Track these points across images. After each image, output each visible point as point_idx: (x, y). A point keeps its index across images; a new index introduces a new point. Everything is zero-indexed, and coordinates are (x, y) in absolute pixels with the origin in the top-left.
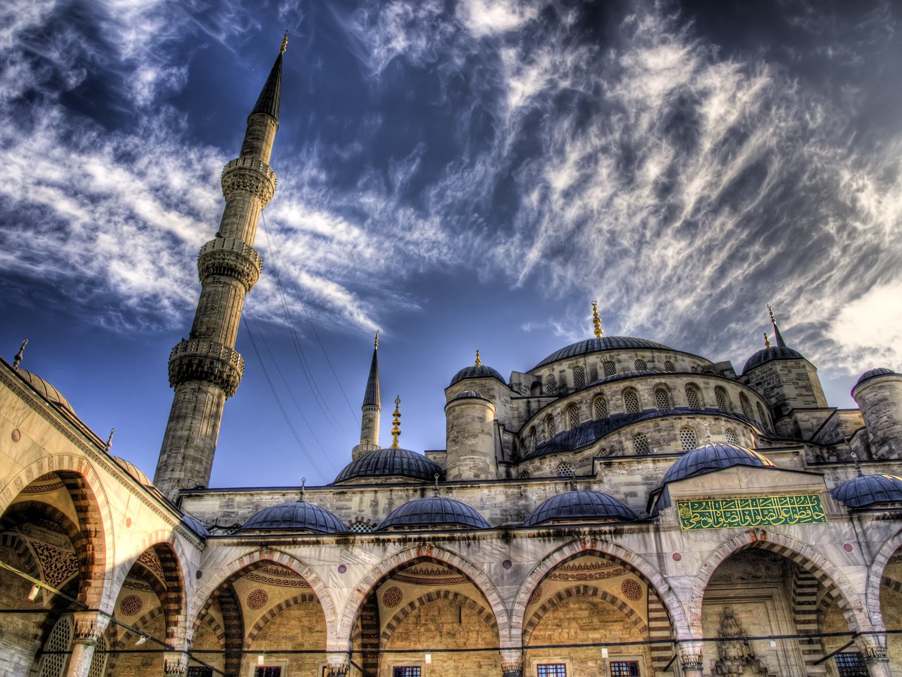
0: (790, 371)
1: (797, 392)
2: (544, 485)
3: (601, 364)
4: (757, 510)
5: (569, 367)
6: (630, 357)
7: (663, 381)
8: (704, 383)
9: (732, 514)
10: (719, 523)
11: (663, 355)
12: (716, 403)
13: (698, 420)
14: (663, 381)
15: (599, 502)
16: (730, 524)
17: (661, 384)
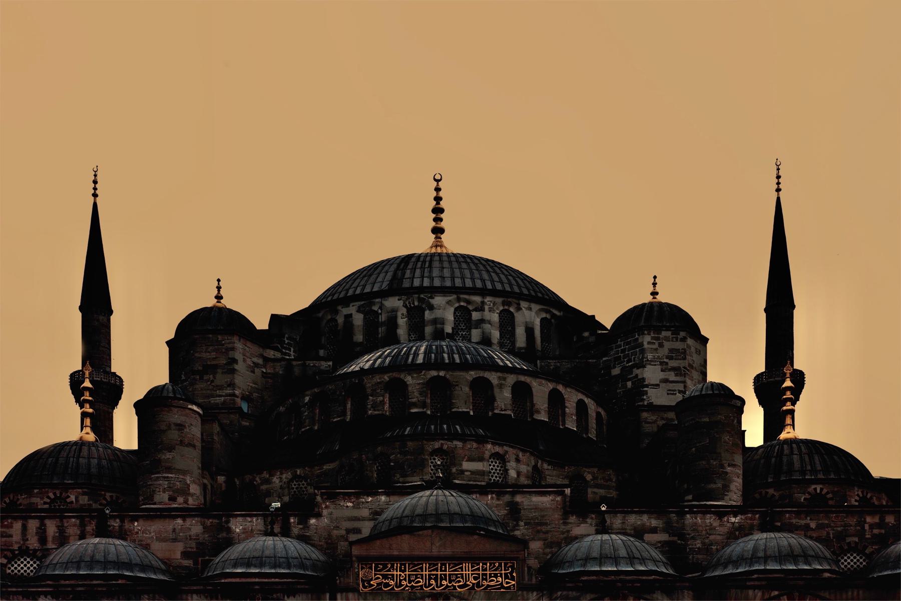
0: (661, 345)
1: (662, 375)
2: (251, 516)
3: (404, 311)
4: (445, 575)
5: (358, 311)
6: (449, 303)
7: (442, 374)
8: (499, 378)
9: (417, 578)
10: (401, 585)
11: (499, 300)
12: (509, 407)
13: (455, 442)
14: (442, 374)
15: (284, 554)
16: (412, 587)
17: (438, 376)
